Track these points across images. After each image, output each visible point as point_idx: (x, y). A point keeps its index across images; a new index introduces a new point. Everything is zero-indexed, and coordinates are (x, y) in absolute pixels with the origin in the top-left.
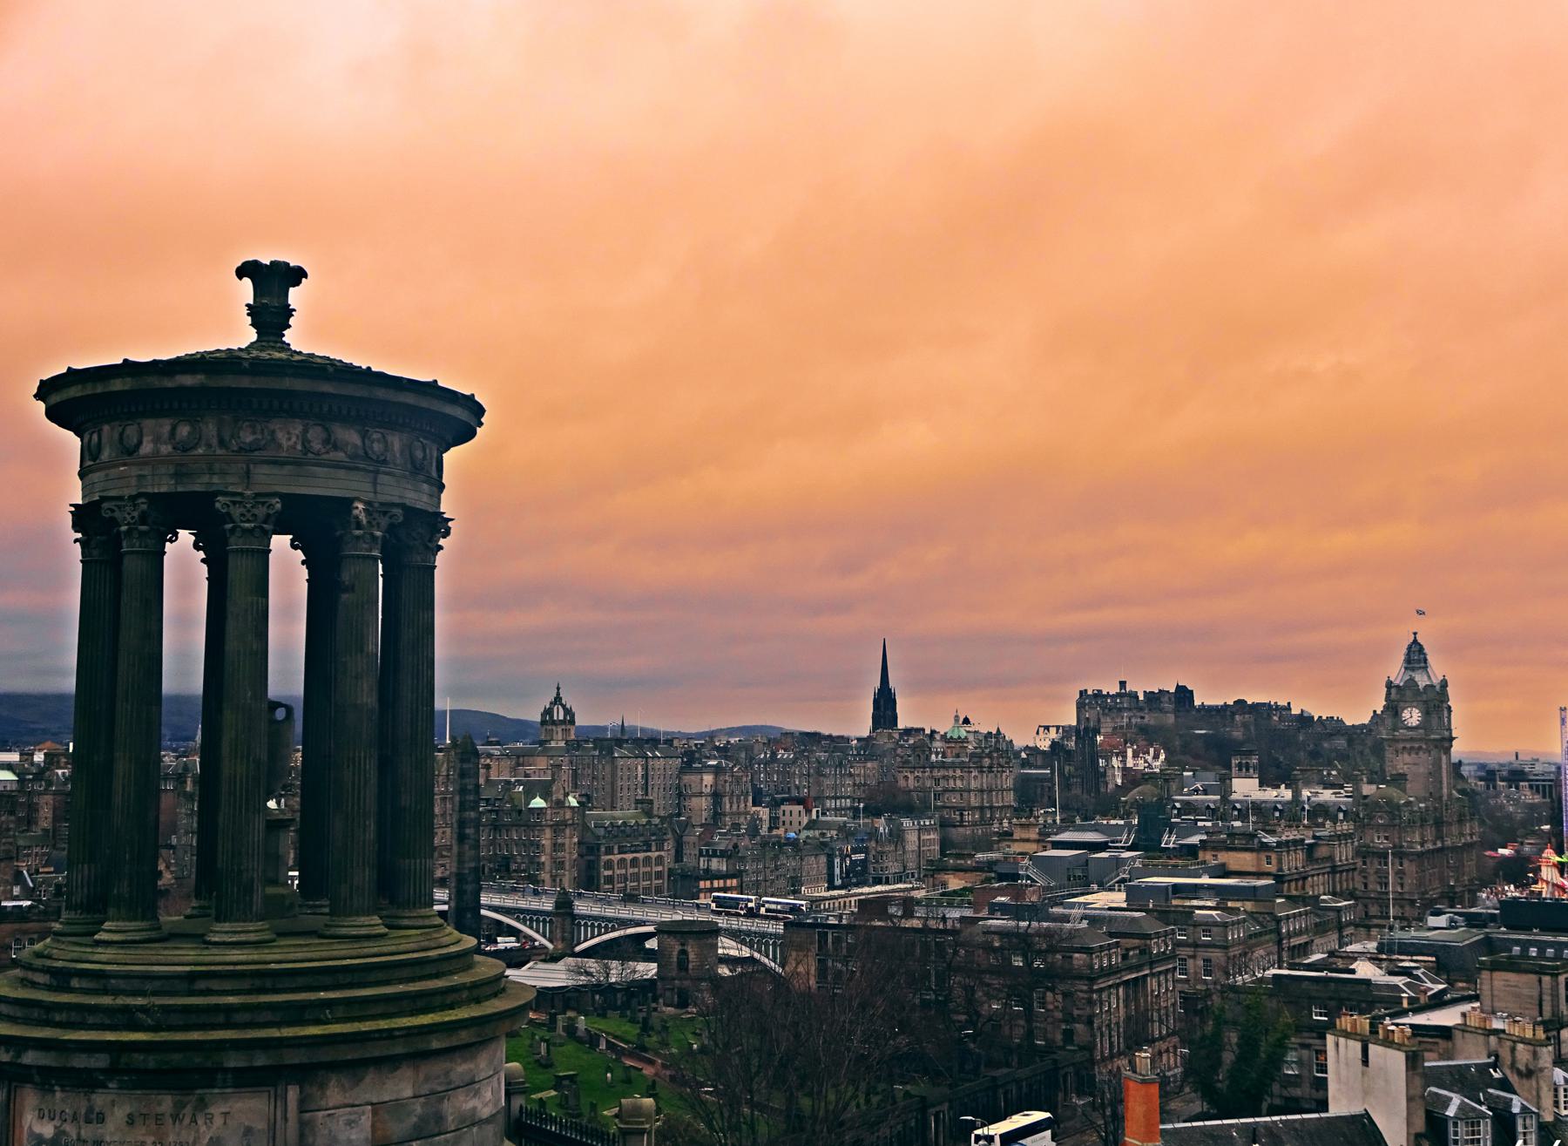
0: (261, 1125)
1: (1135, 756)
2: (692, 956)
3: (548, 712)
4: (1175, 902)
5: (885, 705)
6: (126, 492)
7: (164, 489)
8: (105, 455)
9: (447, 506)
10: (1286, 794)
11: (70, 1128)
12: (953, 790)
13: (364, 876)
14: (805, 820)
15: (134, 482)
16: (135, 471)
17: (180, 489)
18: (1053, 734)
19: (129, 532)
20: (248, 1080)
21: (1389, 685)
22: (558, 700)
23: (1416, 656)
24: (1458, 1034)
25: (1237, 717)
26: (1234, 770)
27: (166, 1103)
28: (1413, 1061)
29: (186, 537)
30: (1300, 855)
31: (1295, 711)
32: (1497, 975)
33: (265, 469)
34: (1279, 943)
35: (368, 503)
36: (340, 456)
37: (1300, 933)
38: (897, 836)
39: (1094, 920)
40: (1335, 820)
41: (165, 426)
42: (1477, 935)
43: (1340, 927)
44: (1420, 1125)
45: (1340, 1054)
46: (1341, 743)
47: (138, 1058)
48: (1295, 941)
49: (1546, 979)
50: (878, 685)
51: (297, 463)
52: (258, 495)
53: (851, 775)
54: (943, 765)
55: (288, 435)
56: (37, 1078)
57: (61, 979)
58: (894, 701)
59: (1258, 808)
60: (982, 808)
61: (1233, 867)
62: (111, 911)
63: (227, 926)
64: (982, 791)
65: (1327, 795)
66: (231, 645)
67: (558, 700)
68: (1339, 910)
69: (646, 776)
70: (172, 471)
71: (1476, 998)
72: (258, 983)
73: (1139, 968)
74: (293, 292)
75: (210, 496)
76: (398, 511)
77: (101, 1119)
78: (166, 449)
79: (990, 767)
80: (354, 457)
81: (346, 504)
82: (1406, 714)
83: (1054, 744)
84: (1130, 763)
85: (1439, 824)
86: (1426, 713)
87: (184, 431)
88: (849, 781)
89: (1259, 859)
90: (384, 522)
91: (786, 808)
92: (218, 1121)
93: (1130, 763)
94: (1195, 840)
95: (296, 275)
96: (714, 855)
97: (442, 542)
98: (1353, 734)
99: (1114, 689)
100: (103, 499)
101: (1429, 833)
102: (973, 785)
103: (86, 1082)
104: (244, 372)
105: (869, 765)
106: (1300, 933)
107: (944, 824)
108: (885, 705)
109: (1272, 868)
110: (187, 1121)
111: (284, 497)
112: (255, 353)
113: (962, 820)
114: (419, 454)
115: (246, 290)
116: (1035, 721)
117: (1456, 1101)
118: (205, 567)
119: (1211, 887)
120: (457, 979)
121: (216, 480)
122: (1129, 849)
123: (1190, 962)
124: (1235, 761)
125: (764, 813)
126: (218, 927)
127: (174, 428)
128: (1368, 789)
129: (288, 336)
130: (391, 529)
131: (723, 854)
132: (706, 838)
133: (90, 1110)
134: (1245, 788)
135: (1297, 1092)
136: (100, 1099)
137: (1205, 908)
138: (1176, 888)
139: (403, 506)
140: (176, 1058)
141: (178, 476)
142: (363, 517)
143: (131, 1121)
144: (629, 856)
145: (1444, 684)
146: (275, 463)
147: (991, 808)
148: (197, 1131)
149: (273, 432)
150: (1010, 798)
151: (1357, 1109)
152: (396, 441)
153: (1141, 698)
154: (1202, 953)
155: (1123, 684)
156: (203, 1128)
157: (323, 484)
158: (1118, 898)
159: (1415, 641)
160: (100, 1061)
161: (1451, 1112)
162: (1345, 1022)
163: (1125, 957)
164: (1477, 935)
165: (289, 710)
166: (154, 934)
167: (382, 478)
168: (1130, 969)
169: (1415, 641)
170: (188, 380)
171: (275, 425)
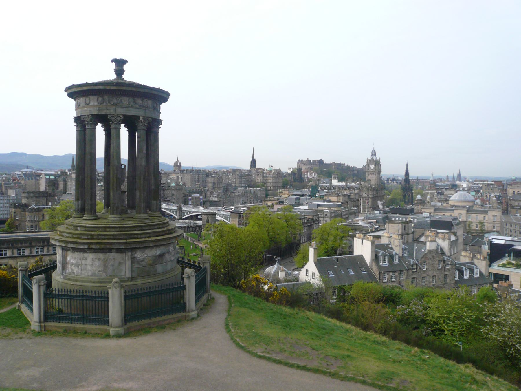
1: (310, 174)
3: (175, 164)
4: (319, 208)
5: (253, 162)
7: (96, 113)
8: (82, 105)
9: (162, 117)
11: (79, 261)
13: (143, 205)
15: (88, 111)
16: (89, 109)
18: (292, 170)
19: (88, 123)
20: (118, 251)
21: (368, 160)
22: (178, 161)
23: (374, 153)
24: (382, 237)
27: (101, 256)
28: (373, 243)
29: (99, 125)
30: (347, 197)
31: (346, 165)
32: (390, 224)
35: (144, 117)
36: (137, 106)
37: (346, 215)
39: (301, 212)
40: (354, 190)
41: (95, 98)
42: (385, 215)
44: (374, 258)
45: (357, 242)
46: (356, 172)
47: (94, 247)
48: (345, 217)
49: (400, 225)
51: (127, 107)
54: (266, 177)
55: (125, 100)
57: (75, 227)
58: (255, 162)
59: (339, 187)
61: (332, 200)
62: (86, 213)
63: (113, 216)
65: (353, 184)
66: (112, 151)
67: (178, 161)
69: (198, 179)
71: (385, 229)
72: (121, 229)
73: (311, 223)
74: (125, 66)
75: (106, 115)
76: (150, 119)
77: (86, 259)
78: (96, 104)
80: (140, 106)
81: (138, 117)
83: (292, 172)
84: (309, 176)
85: (377, 190)
86: (375, 166)
87: (100, 99)
90: (147, 122)
94: (324, 194)
95: (124, 62)
96: (214, 197)
97: (160, 126)
98: (359, 170)
99: (306, 159)
100: (81, 116)
101: (375, 192)
103: (83, 251)
104: (115, 86)
106: (346, 215)
108: (253, 162)
109: (341, 200)
111: (123, 115)
112: (117, 81)
114: (155, 105)
115: (113, 66)
116: (287, 167)
117: (381, 252)
118: (104, 132)
119: (327, 205)
120: (165, 229)
121: (108, 111)
122: (310, 196)
123: (322, 222)
126: (110, 216)
127: (98, 99)
128: (362, 183)
129: (124, 77)
130: (149, 123)
132: (212, 193)
133: (84, 257)
134: (335, 182)
135: (345, 250)
136: (86, 255)
137: (326, 210)
138: (319, 205)
139: (152, 118)
141: (99, 110)
142: (143, 121)
143: (93, 260)
145: (380, 160)
146: (122, 107)
149: (121, 100)
150: (282, 184)
151: (360, 254)
152: (149, 103)
154: (325, 219)
155: (308, 158)
157: (133, 112)
158: (306, 207)
161: (380, 254)
162: (358, 235)
163: (308, 220)
164: (385, 215)
165: (125, 166)
166: (96, 218)
167: (147, 111)
168: (309, 223)
170: (101, 87)
171: (122, 98)
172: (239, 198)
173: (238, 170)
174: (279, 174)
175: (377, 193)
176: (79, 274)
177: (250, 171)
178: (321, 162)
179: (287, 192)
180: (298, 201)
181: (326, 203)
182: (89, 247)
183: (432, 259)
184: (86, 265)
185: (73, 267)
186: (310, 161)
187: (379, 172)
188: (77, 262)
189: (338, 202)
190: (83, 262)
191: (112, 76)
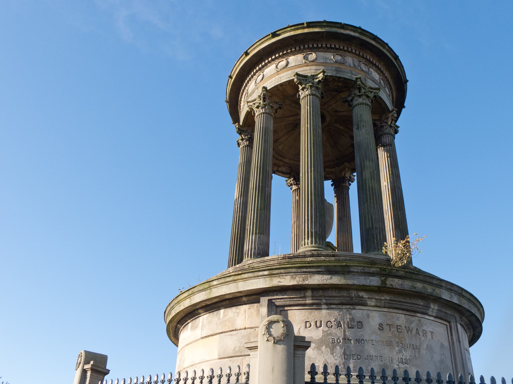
0: (446, 344)
11: (334, 330)
17: (338, 75)
27: (401, 319)
33: (370, 81)
52: (370, 88)
70: (334, 69)
77: (360, 324)
87: (339, 58)
92: (429, 336)
110: (414, 331)
133: (352, 320)
136: (359, 313)
141: (337, 70)
143: (381, 327)
148: (420, 339)
156: (423, 338)
184: (359, 341)
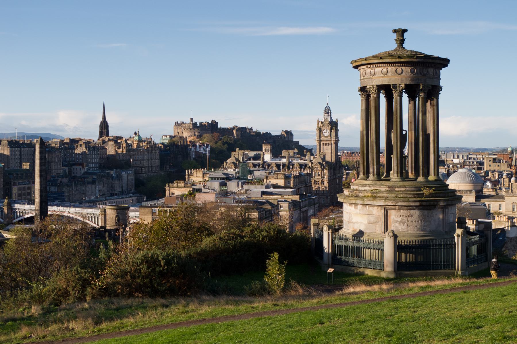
2: (121, 218)
5: (104, 127)
6: (398, 83)
8: (389, 74)
10: (284, 160)
11: (404, 218)
12: (137, 160)
14: (83, 172)
15: (400, 81)
21: (319, 121)
23: (328, 112)
25: (235, 132)
26: (264, 151)
27: (426, 212)
31: (254, 130)
34: (300, 210)
38: (119, 177)
43: (314, 204)
48: (305, 209)
50: (101, 119)
53: (98, 154)
56: (397, 209)
58: (107, 126)
60: (148, 167)
64: (148, 160)
68: (314, 199)
69: (21, 155)
79: (152, 151)
82: (325, 131)
84: (198, 149)
85: (334, 169)
86: (331, 131)
88: (98, 156)
89: (285, 182)
91: (75, 167)
93: (198, 149)
96: (52, 185)
102: (146, 157)
105: (104, 150)
107: (136, 173)
108: (104, 127)
113: (142, 172)
124: (264, 148)
125: (66, 169)
128: (312, 158)
129: (404, 45)
131: (56, 185)
133: (410, 214)
136: (412, 212)
138: (263, 193)
140: (432, 203)
144: (22, 186)
146: (430, 78)
147: (152, 166)
150: (158, 163)
153: (198, 125)
159: (327, 106)
160: (418, 204)
163: (266, 215)
169: (327, 106)
171: (429, 70)
172: (93, 186)
173: (81, 140)
174: (153, 146)
175: (334, 174)
176: (405, 230)
177: (104, 142)
178: (214, 125)
179: (200, 174)
180: (224, 188)
181: (272, 189)
182: (420, 204)
183: (513, 249)
185: (397, 225)
186: (196, 124)
187: (336, 143)
188: (402, 220)
189: (285, 187)
190: (409, 219)
191: (392, 46)
